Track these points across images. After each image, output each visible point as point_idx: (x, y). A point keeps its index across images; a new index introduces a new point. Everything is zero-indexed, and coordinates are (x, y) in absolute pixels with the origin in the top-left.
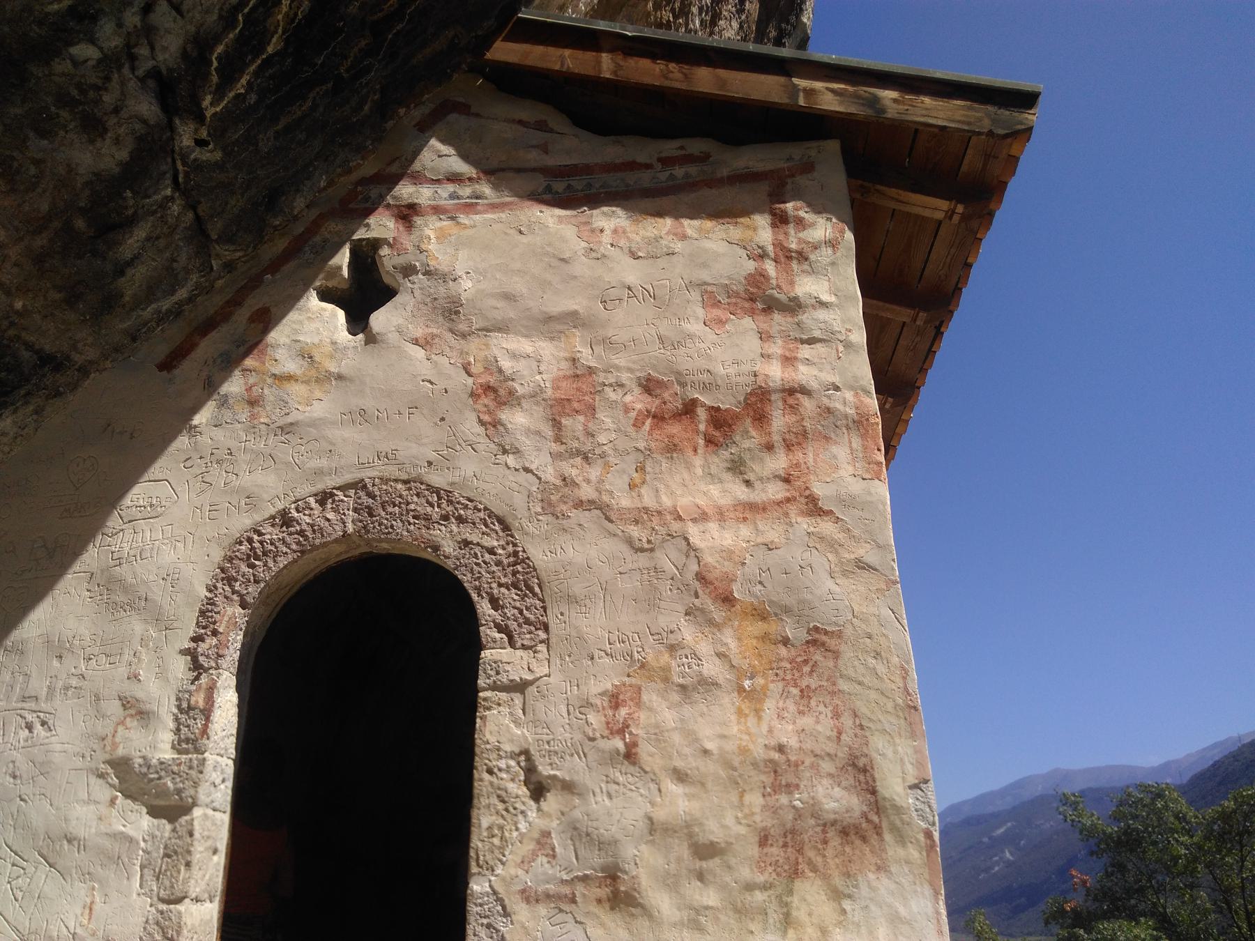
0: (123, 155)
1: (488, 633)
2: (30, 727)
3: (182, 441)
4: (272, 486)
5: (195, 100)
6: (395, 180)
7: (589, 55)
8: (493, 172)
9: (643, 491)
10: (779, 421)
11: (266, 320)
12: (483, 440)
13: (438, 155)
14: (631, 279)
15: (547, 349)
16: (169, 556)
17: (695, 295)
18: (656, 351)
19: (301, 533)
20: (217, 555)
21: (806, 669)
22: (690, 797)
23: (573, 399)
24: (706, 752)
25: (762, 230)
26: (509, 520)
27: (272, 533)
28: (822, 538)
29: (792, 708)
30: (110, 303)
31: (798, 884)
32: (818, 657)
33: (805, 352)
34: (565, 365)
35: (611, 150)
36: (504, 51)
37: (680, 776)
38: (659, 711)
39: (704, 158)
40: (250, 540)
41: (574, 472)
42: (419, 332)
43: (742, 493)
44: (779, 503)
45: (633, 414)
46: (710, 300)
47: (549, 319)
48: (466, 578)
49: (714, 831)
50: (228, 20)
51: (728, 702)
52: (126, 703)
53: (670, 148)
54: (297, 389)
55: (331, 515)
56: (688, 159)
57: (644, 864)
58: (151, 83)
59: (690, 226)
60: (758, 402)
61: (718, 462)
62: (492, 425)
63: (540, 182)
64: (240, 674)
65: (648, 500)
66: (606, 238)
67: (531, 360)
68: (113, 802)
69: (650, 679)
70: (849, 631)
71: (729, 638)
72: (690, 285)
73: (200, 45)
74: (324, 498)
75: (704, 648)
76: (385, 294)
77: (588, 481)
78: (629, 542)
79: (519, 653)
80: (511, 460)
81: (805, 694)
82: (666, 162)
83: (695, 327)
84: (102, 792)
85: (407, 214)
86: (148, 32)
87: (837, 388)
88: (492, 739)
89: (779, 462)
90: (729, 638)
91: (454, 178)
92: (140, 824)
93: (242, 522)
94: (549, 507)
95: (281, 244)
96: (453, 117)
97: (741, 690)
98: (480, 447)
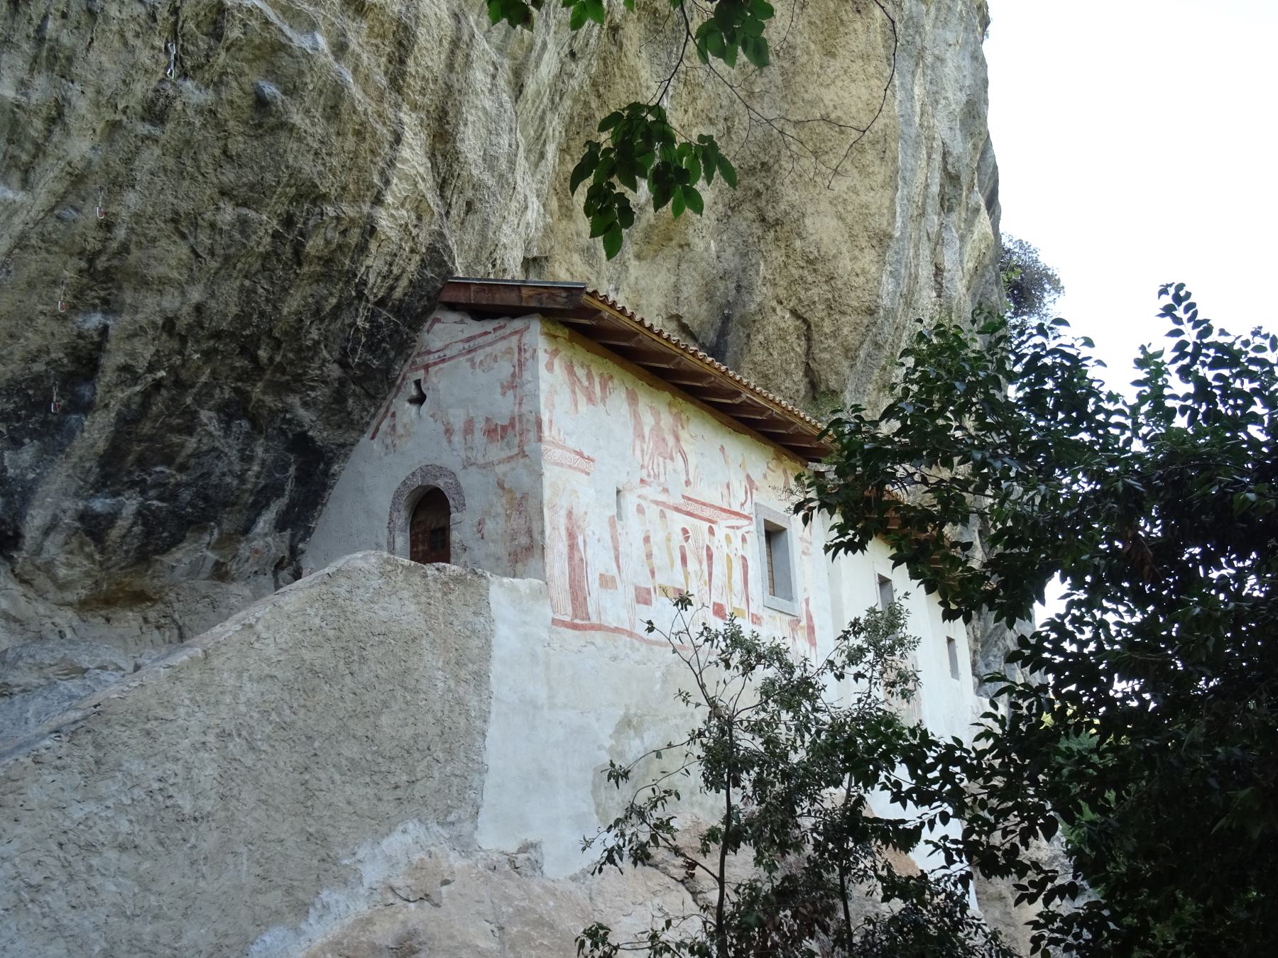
1: (452, 509)
23: (469, 428)
37: (493, 541)
46: (503, 387)
53: (495, 323)
83: (498, 396)
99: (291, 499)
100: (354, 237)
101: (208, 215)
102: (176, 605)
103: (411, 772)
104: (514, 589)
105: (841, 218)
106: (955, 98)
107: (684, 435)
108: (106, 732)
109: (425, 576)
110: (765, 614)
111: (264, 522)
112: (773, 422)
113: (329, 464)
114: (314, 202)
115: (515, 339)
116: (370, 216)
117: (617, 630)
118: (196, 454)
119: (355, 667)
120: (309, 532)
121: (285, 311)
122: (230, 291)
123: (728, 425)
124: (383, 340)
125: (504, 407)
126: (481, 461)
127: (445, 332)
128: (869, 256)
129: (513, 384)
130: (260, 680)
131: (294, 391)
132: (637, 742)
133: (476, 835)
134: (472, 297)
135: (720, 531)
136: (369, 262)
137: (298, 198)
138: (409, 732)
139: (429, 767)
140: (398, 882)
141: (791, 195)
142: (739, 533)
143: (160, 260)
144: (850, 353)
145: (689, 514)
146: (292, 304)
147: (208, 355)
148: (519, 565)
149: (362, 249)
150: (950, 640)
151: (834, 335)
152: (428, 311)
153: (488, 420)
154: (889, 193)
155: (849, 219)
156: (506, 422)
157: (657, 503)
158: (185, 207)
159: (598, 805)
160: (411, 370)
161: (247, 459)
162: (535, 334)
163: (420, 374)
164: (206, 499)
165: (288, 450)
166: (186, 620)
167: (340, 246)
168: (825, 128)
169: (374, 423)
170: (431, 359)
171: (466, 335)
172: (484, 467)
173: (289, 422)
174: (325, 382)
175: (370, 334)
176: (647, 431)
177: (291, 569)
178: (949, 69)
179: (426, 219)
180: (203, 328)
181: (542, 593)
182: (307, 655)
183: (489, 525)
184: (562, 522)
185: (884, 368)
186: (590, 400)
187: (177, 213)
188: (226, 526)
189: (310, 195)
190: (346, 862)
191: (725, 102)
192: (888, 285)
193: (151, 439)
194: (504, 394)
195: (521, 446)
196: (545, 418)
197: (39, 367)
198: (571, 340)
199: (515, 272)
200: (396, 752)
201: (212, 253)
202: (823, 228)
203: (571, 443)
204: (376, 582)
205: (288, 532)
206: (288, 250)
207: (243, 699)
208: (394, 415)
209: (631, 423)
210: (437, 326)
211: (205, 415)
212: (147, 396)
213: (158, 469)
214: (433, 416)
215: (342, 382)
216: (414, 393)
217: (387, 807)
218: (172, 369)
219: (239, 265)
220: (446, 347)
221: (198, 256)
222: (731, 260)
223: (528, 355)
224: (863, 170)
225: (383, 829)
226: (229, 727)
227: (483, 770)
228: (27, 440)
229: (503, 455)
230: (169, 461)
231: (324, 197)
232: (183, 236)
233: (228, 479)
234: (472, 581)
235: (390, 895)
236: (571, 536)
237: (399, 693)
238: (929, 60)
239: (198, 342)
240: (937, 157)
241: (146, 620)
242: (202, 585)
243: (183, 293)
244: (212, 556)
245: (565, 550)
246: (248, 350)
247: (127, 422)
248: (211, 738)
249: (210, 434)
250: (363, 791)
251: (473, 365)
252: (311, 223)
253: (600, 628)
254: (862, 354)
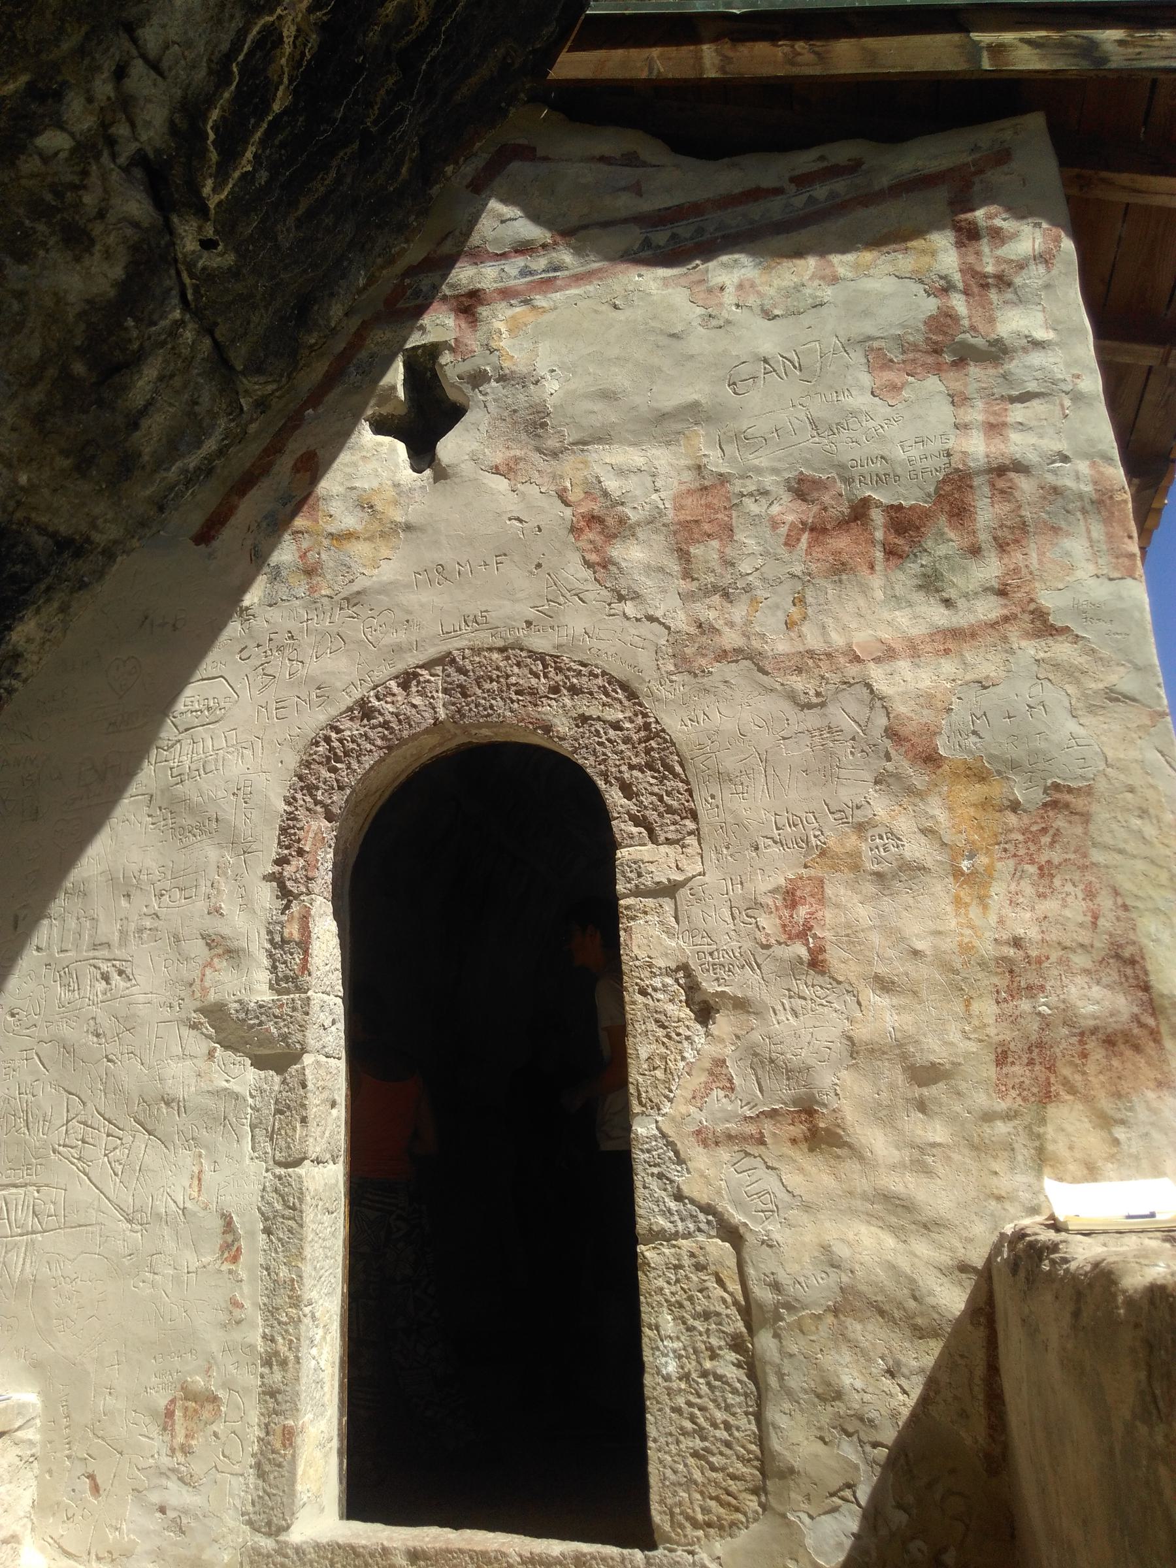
0: (117, 272)
1: (622, 827)
2: (106, 978)
3: (234, 628)
4: (345, 671)
5: (194, 188)
6: (449, 263)
7: (686, 51)
8: (574, 230)
9: (805, 629)
10: (987, 513)
11: (313, 467)
12: (592, 586)
13: (502, 220)
14: (767, 347)
15: (662, 458)
16: (237, 767)
17: (857, 357)
18: (808, 441)
19: (386, 725)
20: (292, 761)
21: (1046, 840)
22: (899, 1009)
23: (702, 521)
24: (916, 953)
25: (943, 252)
26: (635, 685)
27: (352, 728)
28: (1057, 666)
29: (1029, 890)
30: (127, 466)
31: (1052, 1110)
32: (1060, 822)
33: (1017, 413)
34: (688, 476)
35: (726, 178)
36: (574, 65)
37: (884, 985)
38: (849, 907)
39: (854, 167)
40: (328, 740)
41: (712, 615)
42: (498, 457)
43: (940, 616)
44: (993, 625)
45: (783, 530)
46: (878, 360)
47: (663, 417)
48: (588, 763)
49: (934, 1050)
50: (221, 75)
51: (941, 890)
52: (211, 942)
53: (805, 160)
54: (360, 549)
55: (417, 700)
56: (834, 172)
57: (847, 1094)
58: (138, 173)
59: (842, 263)
60: (954, 492)
61: (905, 578)
62: (602, 566)
63: (634, 236)
64: (336, 899)
65: (813, 640)
66: (729, 298)
67: (643, 474)
68: (211, 1055)
69: (835, 868)
70: (1101, 785)
71: (936, 810)
72: (848, 344)
73: (191, 111)
74: (407, 680)
75: (904, 824)
76: (452, 414)
77: (731, 625)
78: (792, 697)
79: (664, 849)
80: (630, 608)
81: (1046, 872)
82: (802, 181)
83: (860, 400)
84: (198, 1045)
85: (469, 305)
86: (125, 104)
87: (1065, 459)
88: (642, 954)
89: (990, 569)
90: (936, 810)
91: (524, 248)
92: (245, 1077)
93: (316, 719)
94: (683, 664)
95: (320, 369)
96: (515, 166)
97: (957, 873)
98: (587, 596)
126: (782, 645)
148: (1069, 1124)
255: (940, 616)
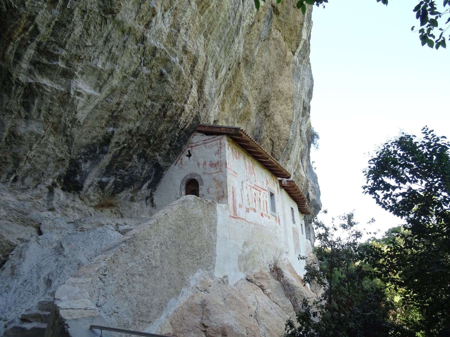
23: (205, 164)
46: (215, 153)
53: (213, 137)
83: (214, 156)
99: (152, 181)
100: (179, 112)
101: (144, 103)
102: (120, 208)
103: (200, 256)
104: (221, 207)
105: (282, 116)
106: (307, 88)
107: (254, 168)
108: (136, 242)
109: (203, 202)
110: (271, 216)
111: (145, 187)
112: (274, 167)
113: (163, 172)
114: (170, 102)
115: (218, 141)
116: (183, 106)
117: (243, 219)
118: (131, 167)
119: (189, 226)
120: (155, 189)
121: (159, 130)
122: (146, 123)
123: (262, 166)
124: (181, 139)
125: (215, 159)
126: (208, 173)
127: (197, 138)
128: (287, 126)
129: (218, 152)
130: (169, 229)
131: (157, 151)
132: (247, 249)
133: (214, 273)
134: (206, 129)
135: (262, 194)
136: (181, 118)
137: (166, 100)
138: (200, 244)
139: (204, 254)
140: (199, 286)
141: (272, 109)
142: (265, 195)
143: (130, 114)
144: (282, 150)
145: (256, 189)
146: (161, 128)
147: (138, 140)
148: (220, 201)
149: (180, 115)
150: (301, 224)
151: (279, 145)
152: (193, 132)
153: (210, 162)
154: (293, 110)
155: (283, 116)
156: (216, 163)
157: (250, 186)
158: (139, 100)
159: (239, 266)
160: (187, 148)
161: (143, 169)
162: (225, 140)
163: (190, 149)
164: (131, 179)
165: (154, 167)
166: (123, 212)
167: (175, 114)
168: (279, 93)
169: (176, 161)
170: (193, 145)
171: (204, 139)
172: (209, 174)
173: (155, 160)
174: (165, 150)
175: (178, 137)
176: (247, 166)
177: (150, 199)
178: (306, 81)
179: (196, 108)
180: (138, 133)
181: (227, 208)
182: (179, 223)
183: (211, 190)
184: (231, 189)
185: (288, 155)
186: (236, 158)
187: (136, 102)
188: (135, 187)
189: (170, 100)
190: (187, 280)
191: (260, 85)
192: (291, 134)
193: (120, 162)
194: (215, 155)
195: (220, 169)
196: (227, 162)
197: (95, 141)
198: (232, 142)
199: (212, 123)
200: (197, 250)
201: (144, 113)
202: (278, 118)
203: (233, 169)
204: (193, 204)
205: (150, 189)
206: (162, 114)
207: (165, 234)
208: (182, 159)
209: (244, 165)
210: (195, 136)
211: (135, 156)
212: (121, 150)
213: (121, 170)
214: (194, 160)
215: (169, 150)
216: (188, 154)
217: (195, 265)
218: (129, 144)
219: (150, 117)
220: (198, 142)
221: (140, 114)
222: (258, 125)
223: (223, 145)
224: (287, 104)
225: (195, 271)
226: (162, 242)
227: (215, 256)
228: (88, 161)
229: (215, 171)
230: (123, 168)
231: (173, 100)
232: (137, 108)
233: (138, 174)
234: (212, 205)
235: (197, 289)
236: (233, 193)
237: (198, 234)
238: (301, 78)
239: (136, 137)
240: (302, 102)
241: (112, 212)
242: (127, 202)
243: (135, 123)
244: (131, 195)
245: (232, 197)
246: (148, 140)
247: (115, 157)
248: (158, 245)
249: (135, 162)
250: (191, 260)
251: (206, 147)
252: (169, 107)
253: (239, 218)
254: (284, 150)
255: (217, 171)
